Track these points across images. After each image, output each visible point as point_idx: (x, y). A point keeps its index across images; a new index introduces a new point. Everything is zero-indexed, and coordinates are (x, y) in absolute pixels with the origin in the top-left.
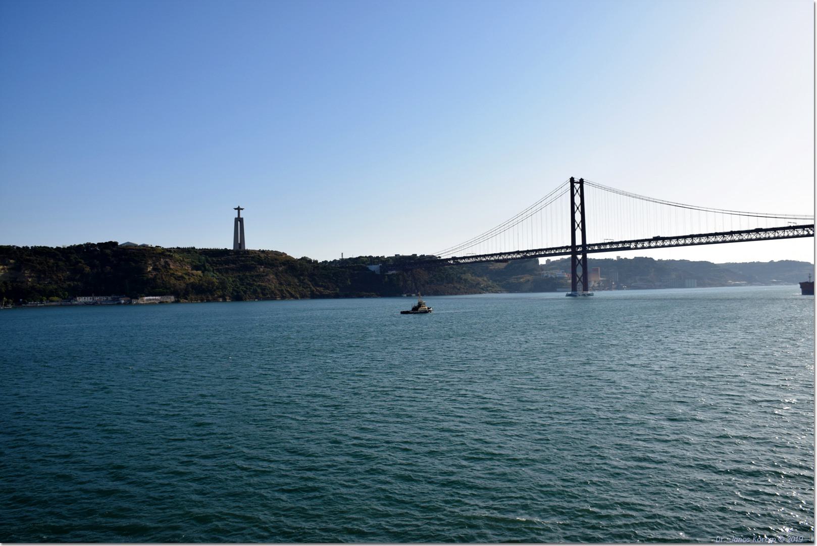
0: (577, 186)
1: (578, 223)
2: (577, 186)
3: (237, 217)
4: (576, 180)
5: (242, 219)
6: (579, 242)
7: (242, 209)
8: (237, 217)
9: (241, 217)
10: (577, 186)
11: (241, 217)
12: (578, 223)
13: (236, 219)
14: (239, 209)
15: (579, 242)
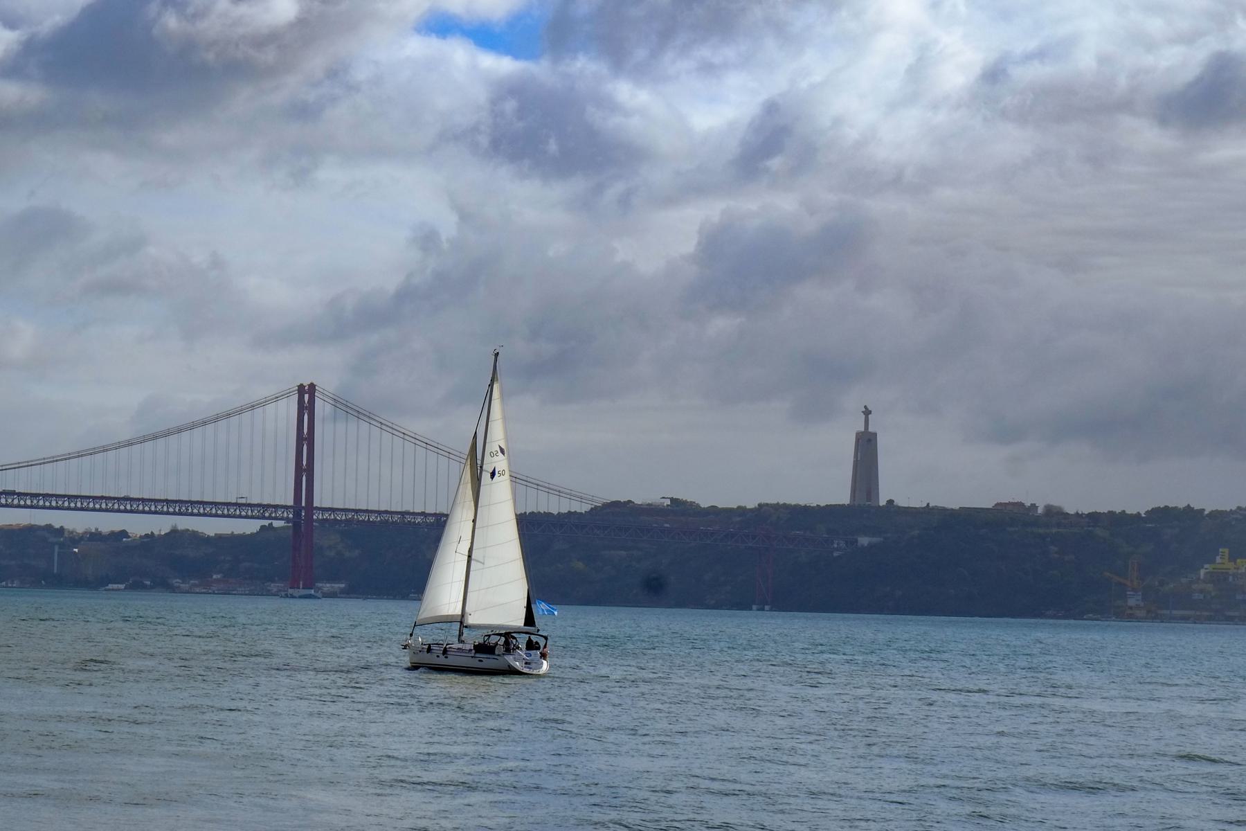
0: (306, 397)
1: (304, 471)
2: (306, 397)
3: (863, 430)
4: (306, 383)
5: (875, 434)
6: (303, 504)
7: (870, 412)
8: (863, 430)
9: (871, 429)
10: (306, 396)
11: (871, 429)
12: (304, 471)
13: (857, 434)
14: (867, 412)
15: (303, 504)
